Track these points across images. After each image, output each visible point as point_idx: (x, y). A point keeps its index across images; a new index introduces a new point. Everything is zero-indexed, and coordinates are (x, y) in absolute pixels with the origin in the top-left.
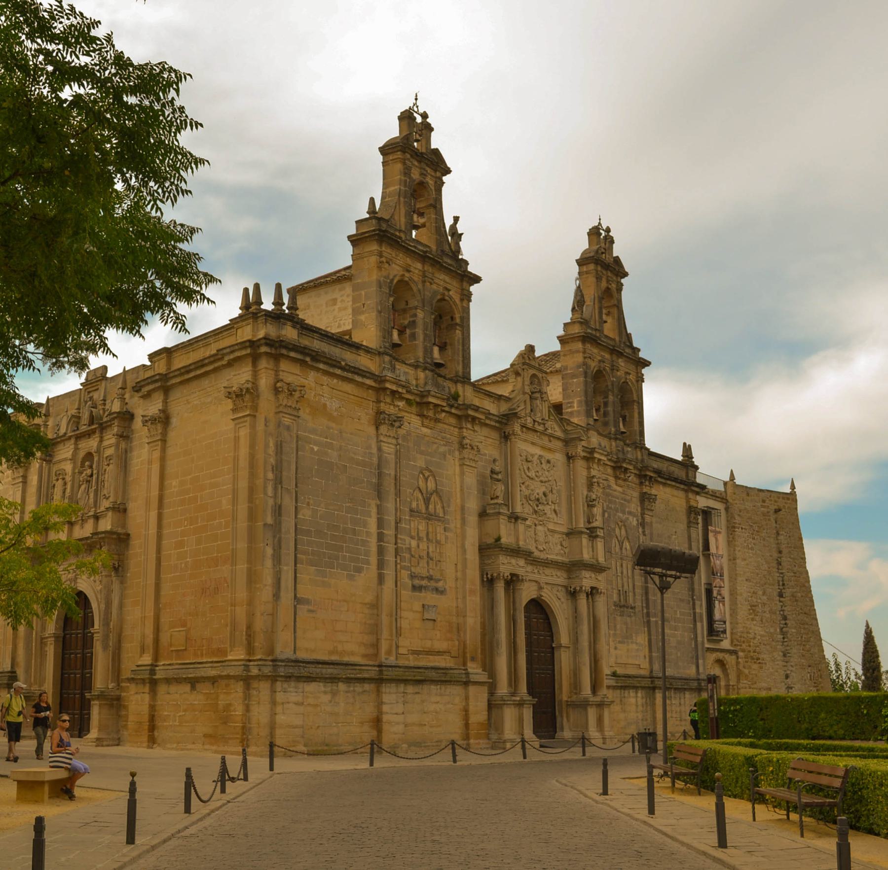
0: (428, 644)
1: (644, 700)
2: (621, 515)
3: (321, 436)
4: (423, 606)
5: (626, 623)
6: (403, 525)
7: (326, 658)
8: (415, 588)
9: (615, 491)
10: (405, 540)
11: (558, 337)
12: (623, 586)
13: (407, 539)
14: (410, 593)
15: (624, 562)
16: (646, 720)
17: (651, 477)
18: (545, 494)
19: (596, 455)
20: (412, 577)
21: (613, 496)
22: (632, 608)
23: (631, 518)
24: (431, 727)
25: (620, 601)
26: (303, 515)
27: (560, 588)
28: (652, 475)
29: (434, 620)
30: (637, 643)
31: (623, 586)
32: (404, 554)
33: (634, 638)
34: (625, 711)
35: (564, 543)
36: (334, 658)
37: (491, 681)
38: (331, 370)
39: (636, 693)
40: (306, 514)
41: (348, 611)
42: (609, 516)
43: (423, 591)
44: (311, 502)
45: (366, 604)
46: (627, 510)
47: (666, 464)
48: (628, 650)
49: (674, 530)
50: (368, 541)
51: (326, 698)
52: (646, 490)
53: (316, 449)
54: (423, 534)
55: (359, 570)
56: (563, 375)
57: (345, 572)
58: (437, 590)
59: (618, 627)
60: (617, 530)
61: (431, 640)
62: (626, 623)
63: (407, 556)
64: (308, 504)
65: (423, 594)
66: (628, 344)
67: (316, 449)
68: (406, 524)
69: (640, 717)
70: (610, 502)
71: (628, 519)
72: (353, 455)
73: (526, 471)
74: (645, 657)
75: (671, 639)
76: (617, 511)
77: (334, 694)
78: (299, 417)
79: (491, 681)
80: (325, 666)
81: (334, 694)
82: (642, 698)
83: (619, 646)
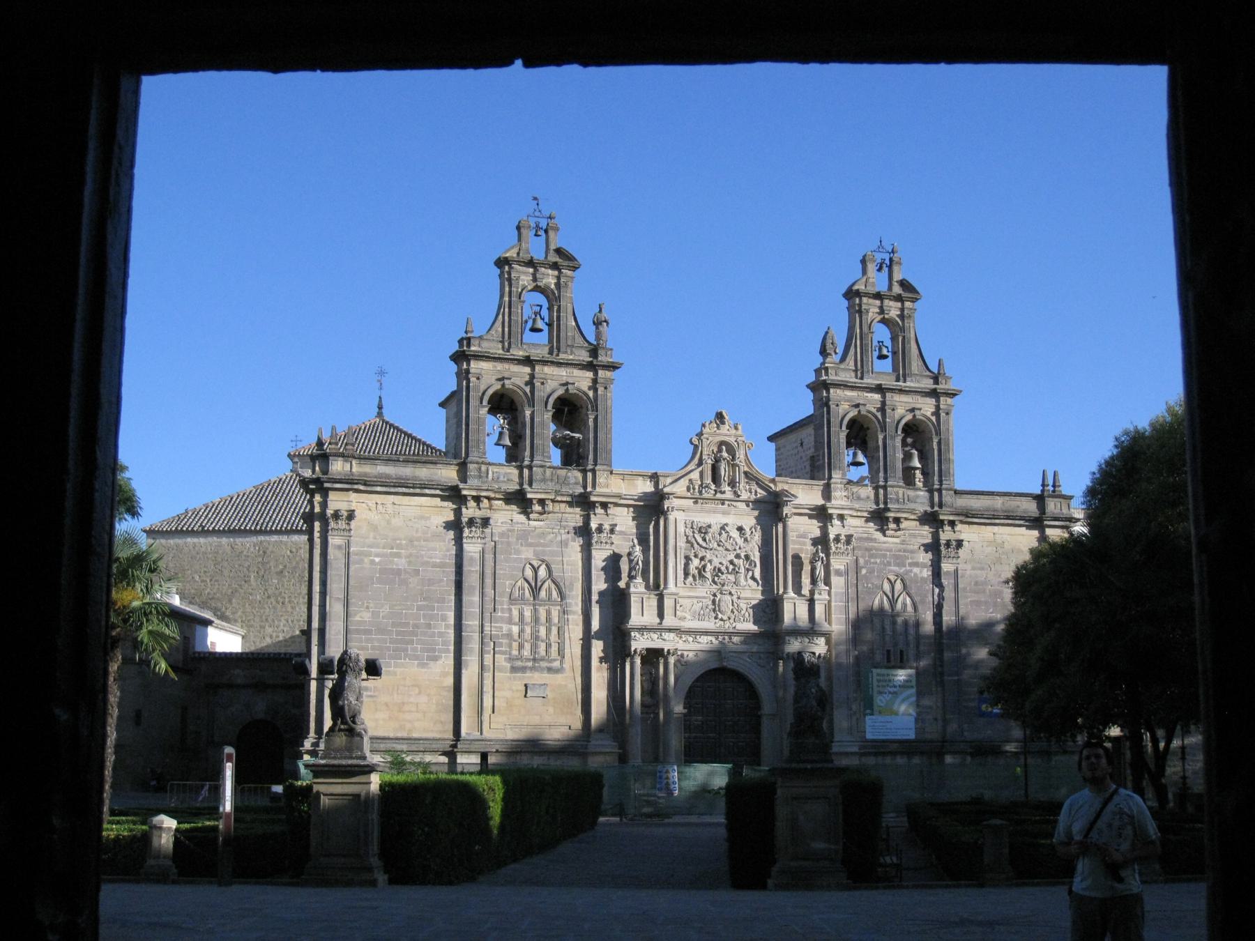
2: (896, 569)
3: (384, 548)
4: (526, 686)
6: (499, 614)
7: (392, 735)
8: (514, 669)
9: (884, 543)
10: (501, 628)
11: (808, 386)
12: (896, 645)
13: (505, 627)
14: (508, 674)
18: (731, 562)
19: (830, 511)
20: (511, 659)
21: (876, 550)
23: (916, 570)
26: (361, 617)
27: (762, 655)
28: (951, 518)
29: (544, 697)
31: (896, 645)
32: (501, 640)
35: (767, 610)
36: (399, 735)
37: (620, 751)
38: (392, 490)
40: (362, 616)
41: (420, 693)
42: (871, 571)
43: (528, 671)
44: (371, 605)
45: (444, 687)
46: (910, 561)
50: (448, 633)
53: (377, 560)
55: (435, 659)
56: (815, 426)
57: (416, 662)
58: (550, 670)
63: (505, 641)
64: (367, 607)
65: (528, 674)
66: (928, 373)
67: (377, 560)
68: (502, 612)
70: (871, 556)
71: (911, 571)
72: (429, 560)
73: (704, 544)
78: (351, 536)
79: (620, 751)
80: (384, 741)
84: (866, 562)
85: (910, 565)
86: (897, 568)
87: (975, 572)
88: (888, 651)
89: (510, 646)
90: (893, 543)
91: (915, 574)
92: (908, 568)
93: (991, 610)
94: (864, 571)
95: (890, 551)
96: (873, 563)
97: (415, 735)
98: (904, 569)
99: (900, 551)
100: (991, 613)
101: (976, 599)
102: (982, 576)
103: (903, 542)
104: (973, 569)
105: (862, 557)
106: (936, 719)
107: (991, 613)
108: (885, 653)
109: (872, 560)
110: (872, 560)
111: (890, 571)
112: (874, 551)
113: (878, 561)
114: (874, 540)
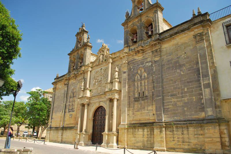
0: (70, 122)
1: (149, 133)
5: (141, 104)
9: (138, 59)
12: (141, 90)
15: (143, 82)
16: (150, 141)
17: (156, 43)
21: (136, 62)
22: (146, 97)
23: (147, 64)
24: (68, 139)
25: (139, 96)
28: (154, 43)
30: (148, 110)
33: (146, 108)
34: (135, 137)
39: (143, 130)
42: (134, 70)
47: (177, 28)
48: (141, 114)
49: (183, 52)
51: (53, 133)
52: (154, 49)
54: (72, 101)
59: (136, 106)
60: (139, 72)
61: (71, 121)
62: (141, 104)
69: (146, 139)
70: (134, 65)
74: (154, 114)
75: (178, 103)
76: (139, 65)
77: (54, 132)
81: (54, 132)
82: (148, 132)
83: (135, 113)
84: (133, 67)
85: (146, 63)
86: (141, 66)
87: (168, 57)
88: (139, 93)
89: (69, 107)
90: (140, 58)
91: (147, 65)
92: (145, 64)
93: (174, 69)
94: (132, 70)
95: (140, 61)
96: (135, 66)
97: (57, 127)
98: (143, 65)
99: (142, 60)
100: (175, 70)
101: (168, 67)
102: (170, 57)
103: (143, 57)
104: (167, 56)
105: (132, 66)
106: (154, 114)
107: (175, 70)
108: (138, 93)
109: (135, 66)
110: (135, 66)
111: (140, 67)
112: (135, 63)
113: (136, 65)
114: (135, 60)
